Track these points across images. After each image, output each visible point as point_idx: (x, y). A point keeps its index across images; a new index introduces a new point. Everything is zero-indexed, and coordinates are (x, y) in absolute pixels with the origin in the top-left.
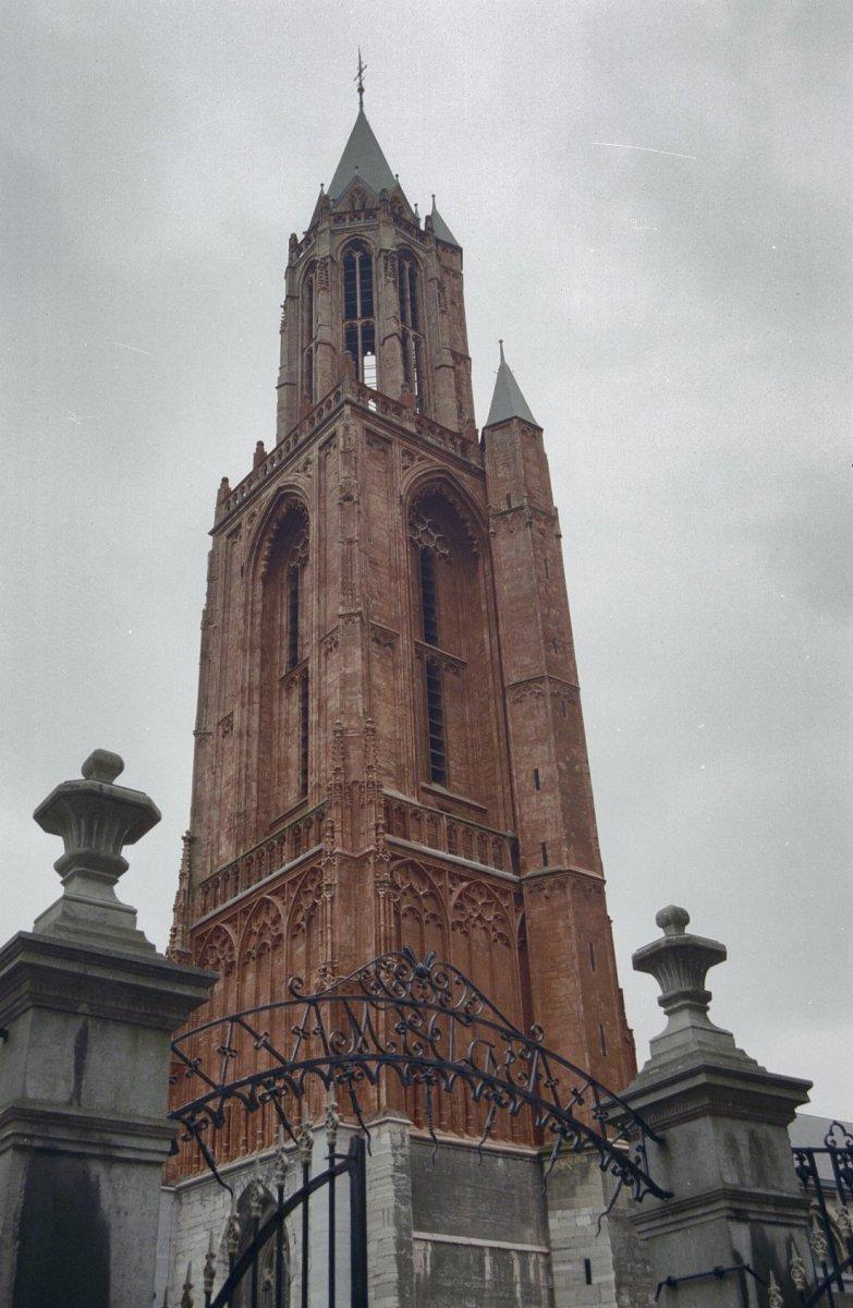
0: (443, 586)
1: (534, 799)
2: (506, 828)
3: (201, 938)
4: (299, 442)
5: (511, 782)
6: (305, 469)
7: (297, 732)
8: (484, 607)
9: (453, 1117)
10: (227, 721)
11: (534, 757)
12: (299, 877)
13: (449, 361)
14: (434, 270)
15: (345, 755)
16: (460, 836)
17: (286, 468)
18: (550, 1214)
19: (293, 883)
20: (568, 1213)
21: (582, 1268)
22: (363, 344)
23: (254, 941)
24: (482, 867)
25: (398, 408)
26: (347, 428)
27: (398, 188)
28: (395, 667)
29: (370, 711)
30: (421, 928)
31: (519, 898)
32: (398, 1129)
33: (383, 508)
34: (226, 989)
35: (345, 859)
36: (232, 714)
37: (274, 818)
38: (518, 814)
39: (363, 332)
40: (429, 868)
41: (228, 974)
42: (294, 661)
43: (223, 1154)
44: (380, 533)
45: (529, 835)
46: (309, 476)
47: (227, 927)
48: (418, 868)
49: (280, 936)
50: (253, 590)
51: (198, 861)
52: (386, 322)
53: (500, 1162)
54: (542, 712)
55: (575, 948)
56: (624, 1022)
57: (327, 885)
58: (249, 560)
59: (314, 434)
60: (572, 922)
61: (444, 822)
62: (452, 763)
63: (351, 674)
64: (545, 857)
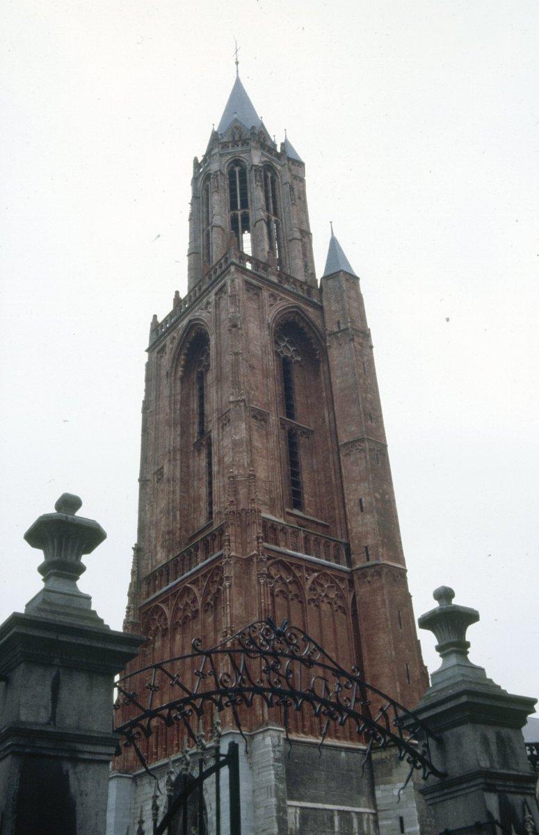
0: (297, 382)
1: (359, 518)
2: (342, 538)
3: (146, 613)
4: (202, 290)
5: (344, 507)
6: (206, 308)
7: (205, 478)
8: (324, 394)
9: (311, 725)
10: (160, 472)
11: (358, 491)
12: (208, 572)
13: (298, 235)
14: (287, 177)
15: (236, 492)
16: (311, 542)
17: (194, 308)
18: (376, 787)
19: (205, 576)
20: (388, 787)
21: (398, 822)
22: (242, 226)
23: (180, 614)
24: (327, 562)
25: (266, 266)
26: (233, 281)
27: (262, 125)
28: (267, 434)
29: (252, 463)
30: (288, 602)
31: (351, 583)
32: (275, 734)
33: (257, 332)
34: (163, 646)
35: (238, 560)
36: (162, 468)
37: (191, 534)
38: (349, 527)
39: (242, 218)
40: (292, 564)
41: (163, 636)
42: (202, 432)
43: (163, 753)
44: (256, 348)
45: (356, 542)
46: (209, 312)
47: (162, 606)
48: (287, 565)
49: (197, 610)
50: (175, 387)
51: (143, 563)
52: (257, 211)
53: (343, 754)
54: (364, 461)
55: (388, 614)
56: (421, 661)
57: (226, 577)
58: (172, 367)
59: (212, 285)
60: (386, 597)
63: (239, 440)
64: (368, 555)
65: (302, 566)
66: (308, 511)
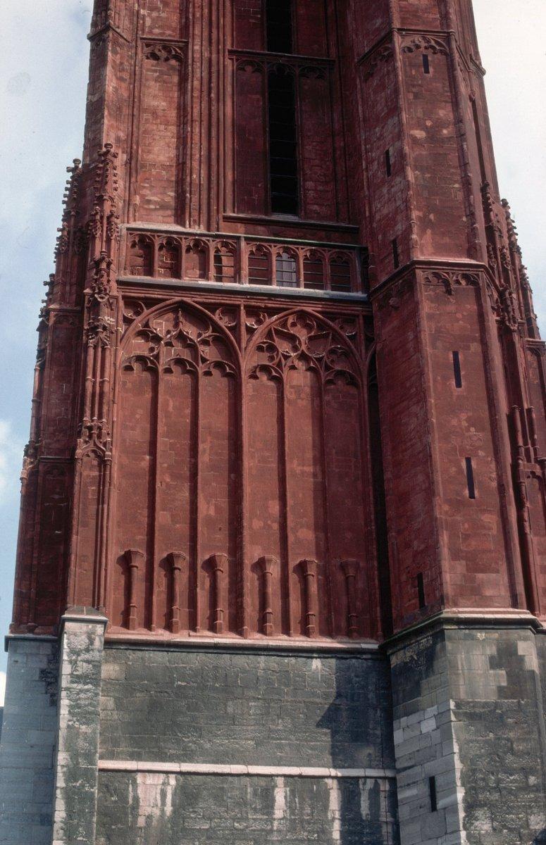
1: (385, 190)
18: (395, 724)
20: (413, 719)
21: (424, 789)
31: (369, 320)
32: (85, 627)
40: (213, 307)
61: (245, 249)
62: (310, 184)
65: (239, 306)
66: (315, 212)
